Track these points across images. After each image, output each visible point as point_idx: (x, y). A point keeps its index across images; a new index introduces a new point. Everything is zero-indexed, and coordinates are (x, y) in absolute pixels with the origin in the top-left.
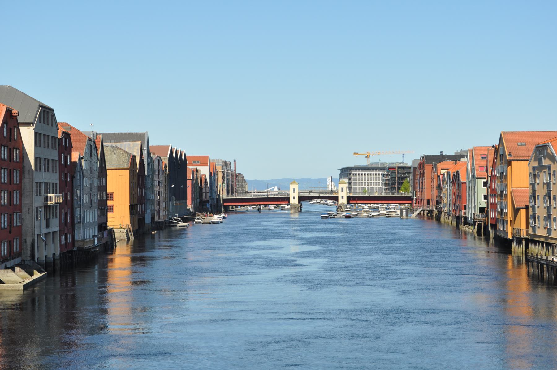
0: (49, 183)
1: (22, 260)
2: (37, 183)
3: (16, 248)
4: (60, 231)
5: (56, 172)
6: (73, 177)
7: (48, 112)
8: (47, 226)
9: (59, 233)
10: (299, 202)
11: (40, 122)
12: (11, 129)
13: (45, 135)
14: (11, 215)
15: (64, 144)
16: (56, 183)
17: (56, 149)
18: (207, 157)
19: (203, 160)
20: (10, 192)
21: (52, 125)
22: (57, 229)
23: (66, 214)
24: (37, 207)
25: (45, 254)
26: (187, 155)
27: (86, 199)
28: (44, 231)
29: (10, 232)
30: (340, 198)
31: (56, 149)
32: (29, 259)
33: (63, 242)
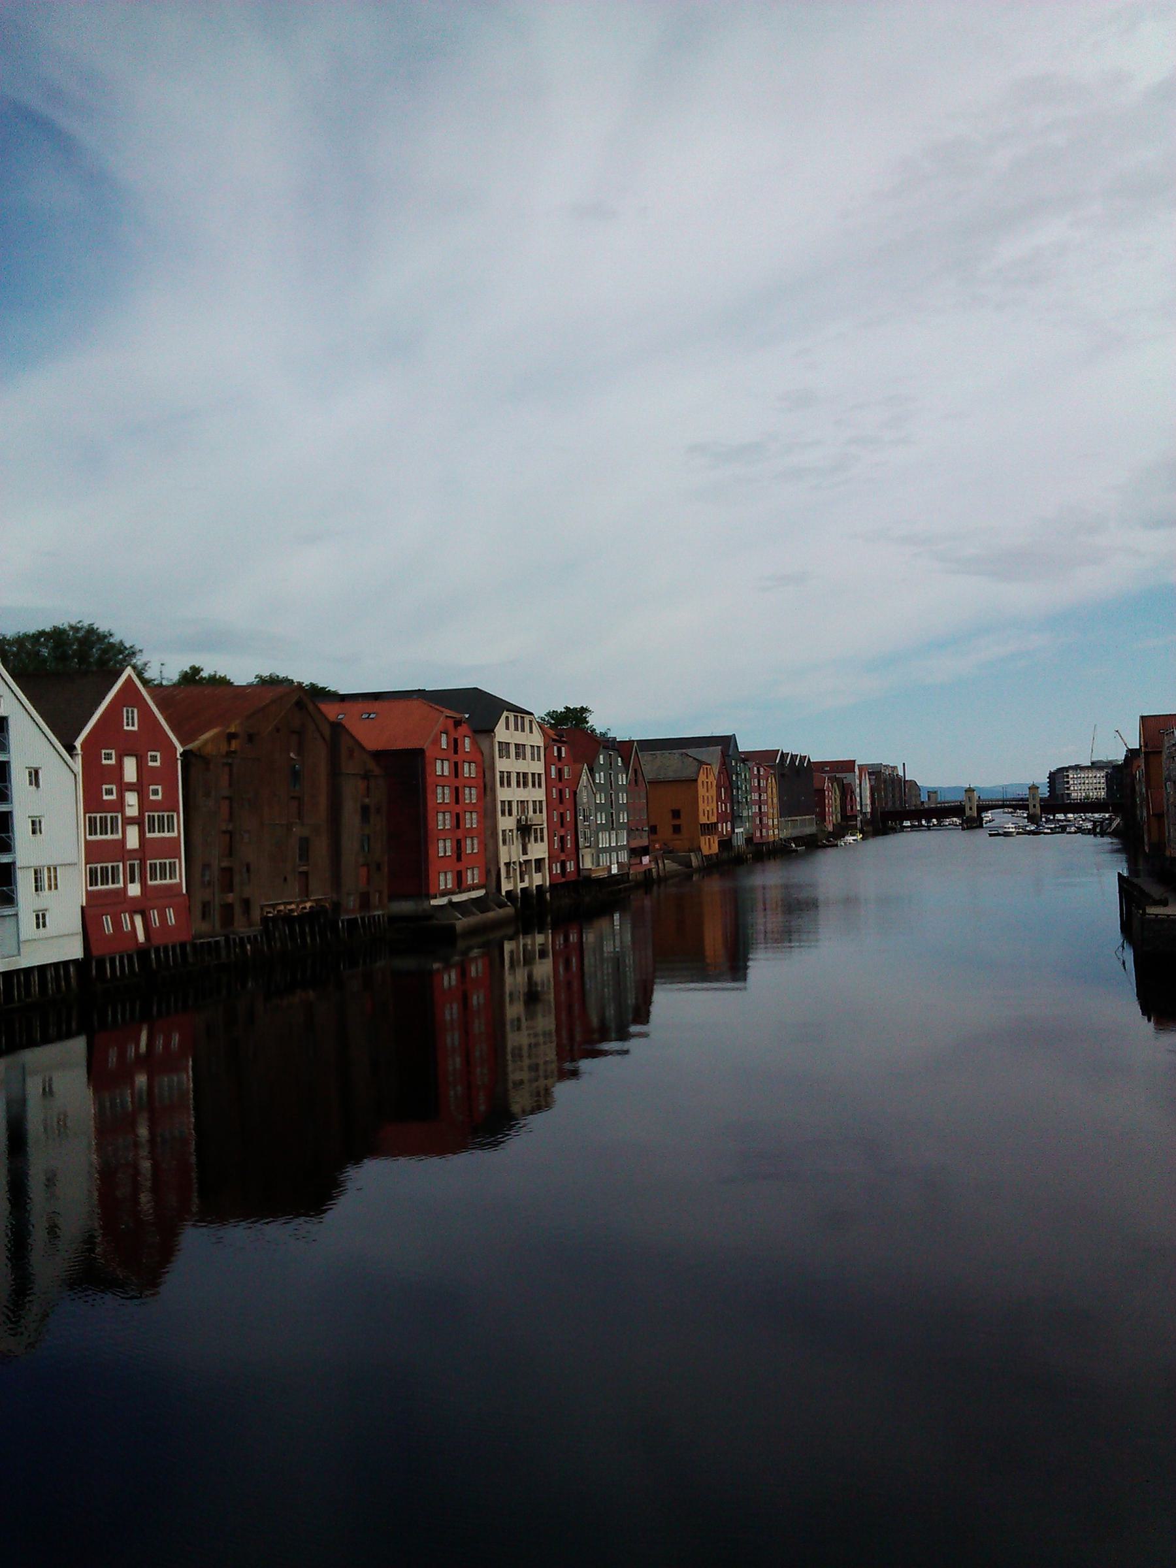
0: (527, 801)
1: (486, 893)
2: (502, 801)
3: (471, 877)
4: (549, 857)
5: (540, 786)
6: (574, 794)
7: (522, 718)
8: (525, 852)
9: (547, 861)
10: (979, 813)
11: (507, 728)
12: (456, 740)
13: (517, 745)
14: (459, 842)
15: (556, 754)
16: (541, 802)
17: (539, 760)
18: (854, 761)
19: (849, 766)
20: (458, 815)
21: (531, 732)
22: (546, 855)
23: (562, 840)
24: (504, 831)
25: (521, 885)
26: (812, 761)
27: (601, 819)
28: (523, 858)
29: (459, 859)
30: (1031, 806)
31: (539, 760)
32: (494, 891)
33: (557, 869)
